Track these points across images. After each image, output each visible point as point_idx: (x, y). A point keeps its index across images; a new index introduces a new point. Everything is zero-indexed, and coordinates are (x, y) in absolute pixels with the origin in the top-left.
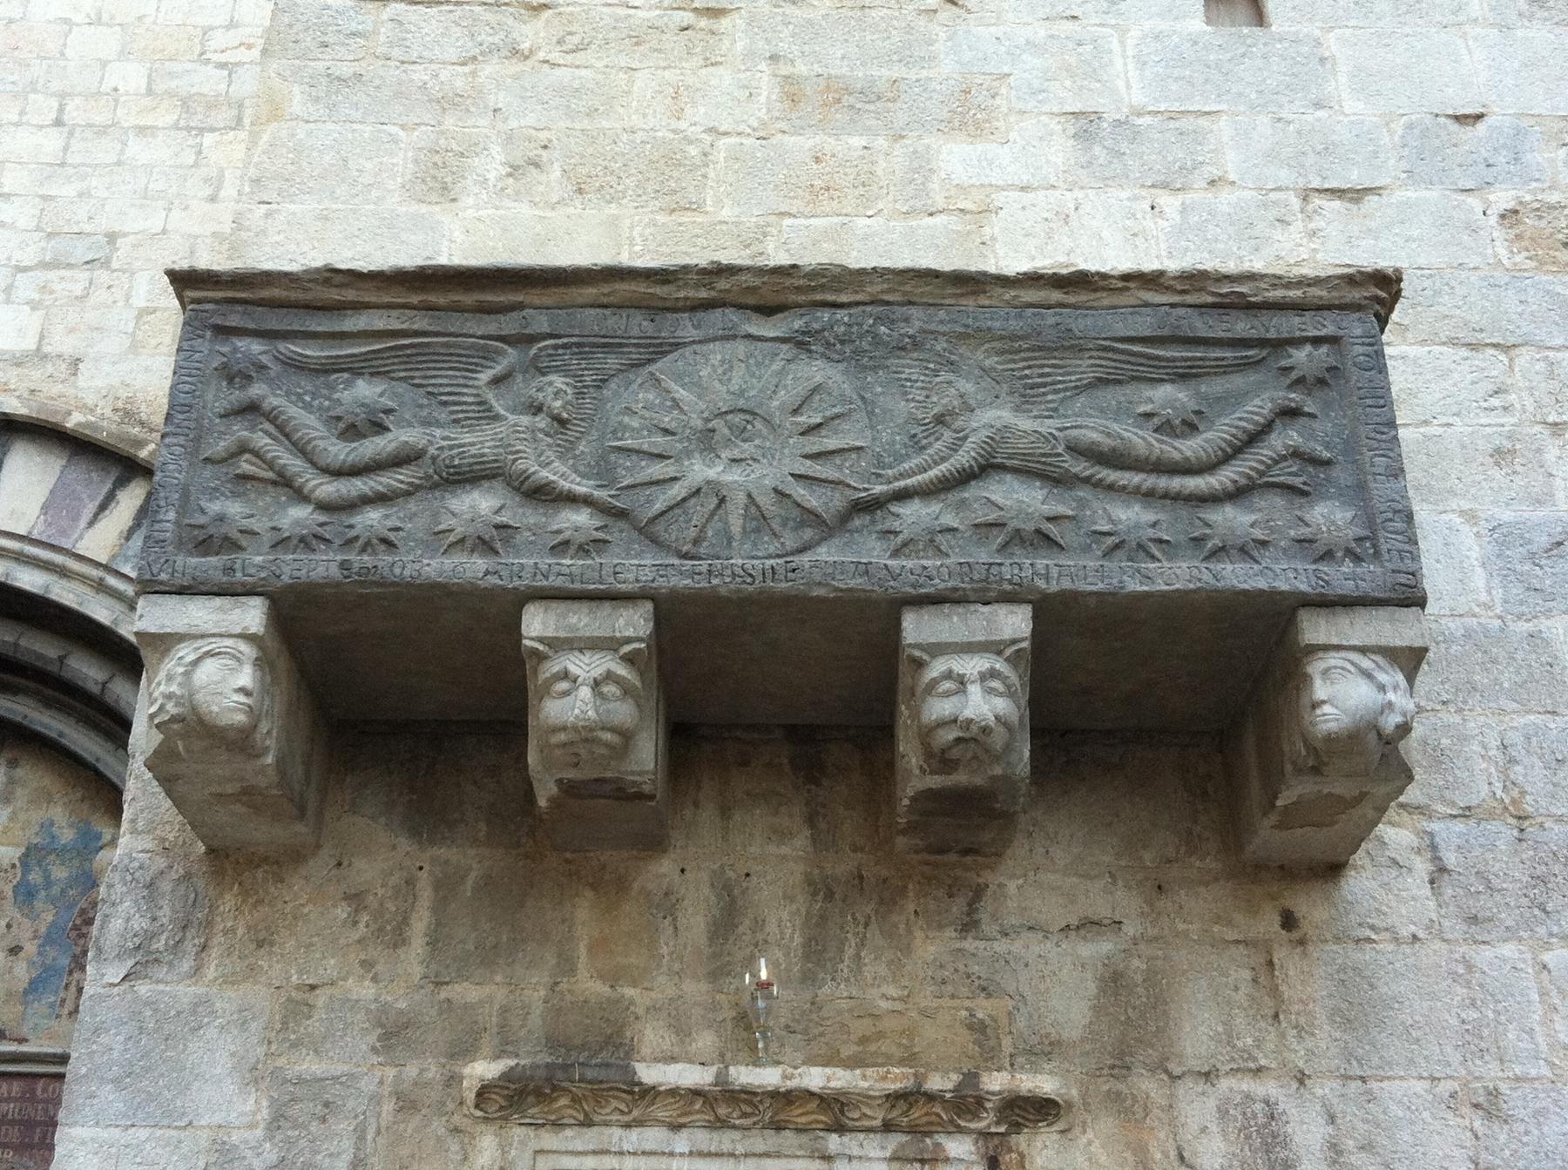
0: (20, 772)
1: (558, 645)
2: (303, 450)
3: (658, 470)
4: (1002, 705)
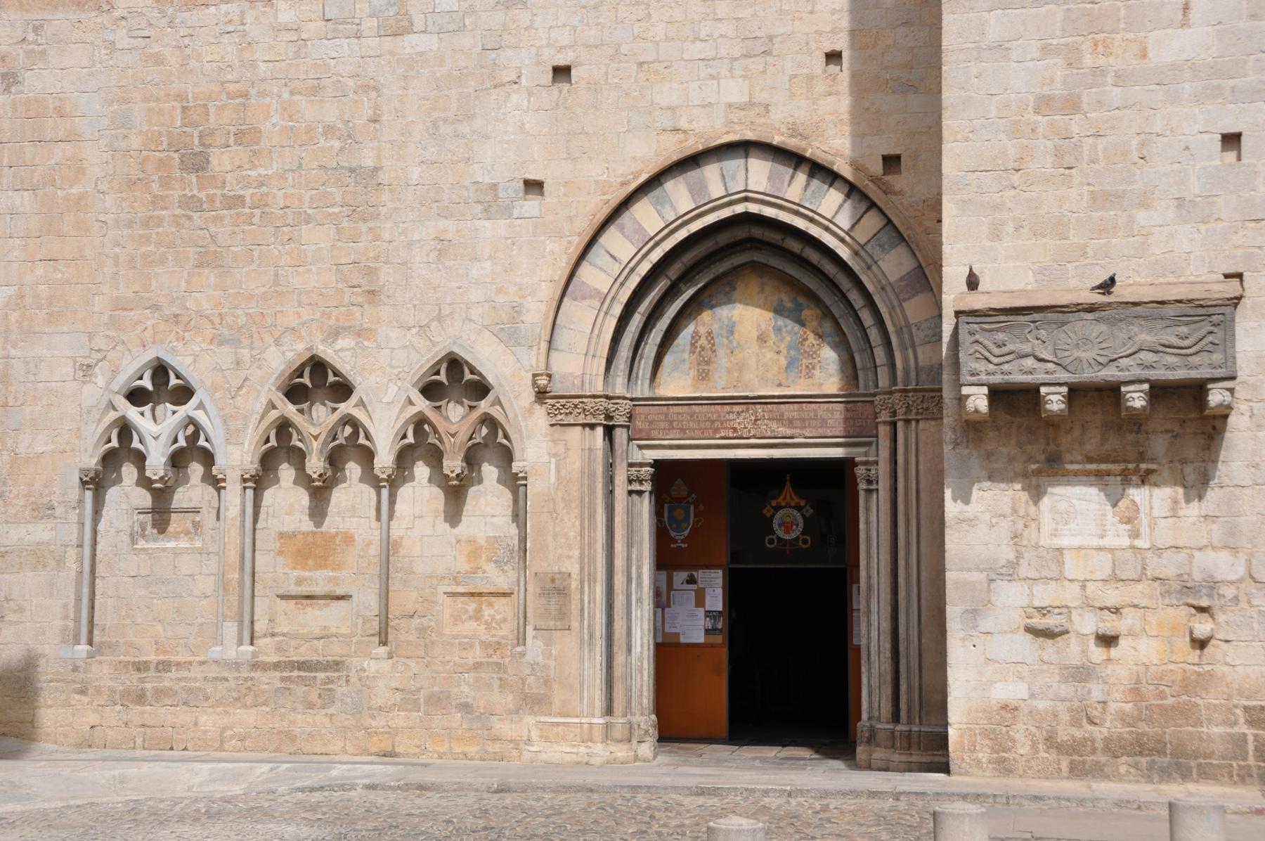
0: (765, 280)
1: (1048, 394)
2: (989, 351)
3: (1066, 354)
4: (1143, 403)
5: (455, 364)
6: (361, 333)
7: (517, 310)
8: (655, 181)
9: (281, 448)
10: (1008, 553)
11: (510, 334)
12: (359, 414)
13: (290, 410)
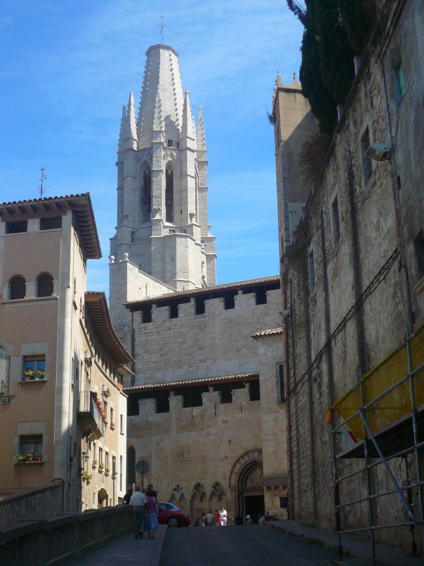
7: (225, 475)
12: (204, 491)
13: (195, 491)
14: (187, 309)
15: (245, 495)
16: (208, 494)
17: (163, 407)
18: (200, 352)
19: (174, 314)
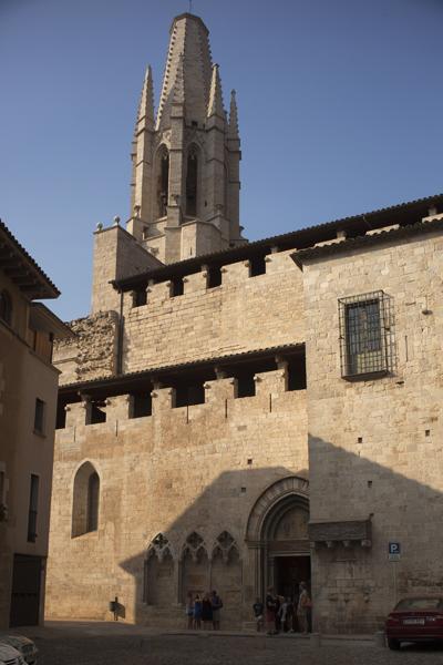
5: (226, 533)
6: (205, 526)
7: (240, 520)
8: (272, 486)
9: (186, 555)
10: (324, 580)
11: (239, 527)
13: (190, 546)
14: (196, 281)
15: (274, 556)
16: (209, 551)
17: (141, 408)
18: (213, 341)
19: (177, 290)
